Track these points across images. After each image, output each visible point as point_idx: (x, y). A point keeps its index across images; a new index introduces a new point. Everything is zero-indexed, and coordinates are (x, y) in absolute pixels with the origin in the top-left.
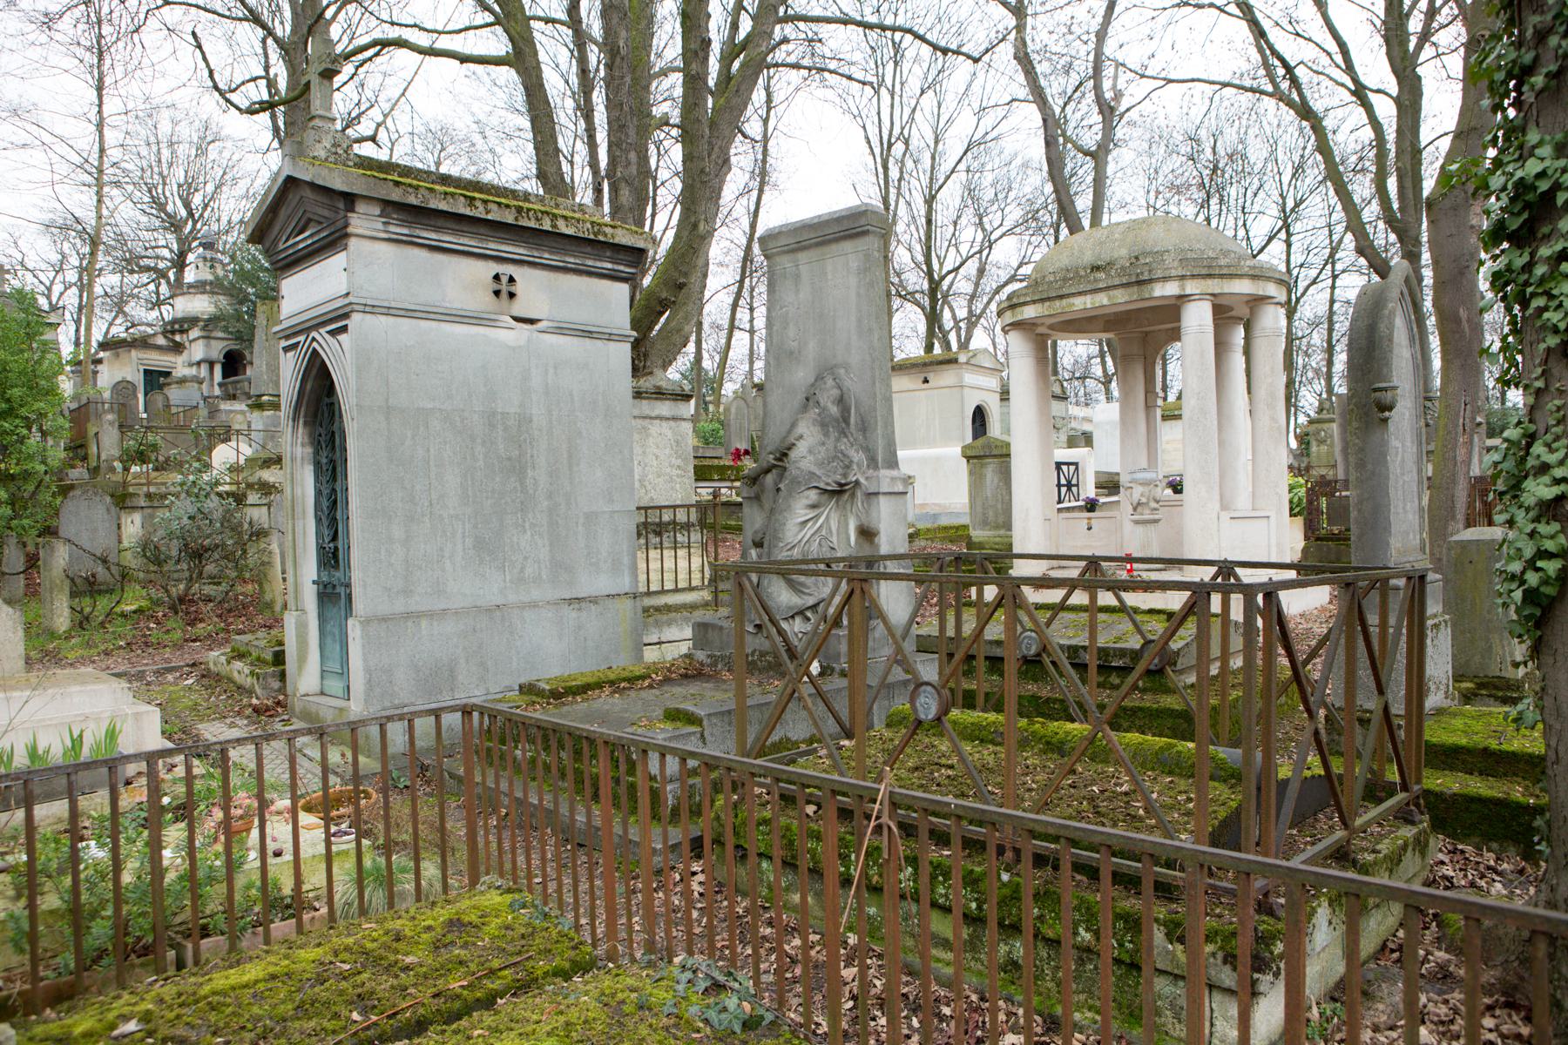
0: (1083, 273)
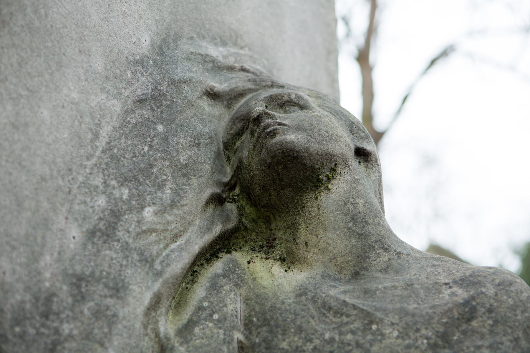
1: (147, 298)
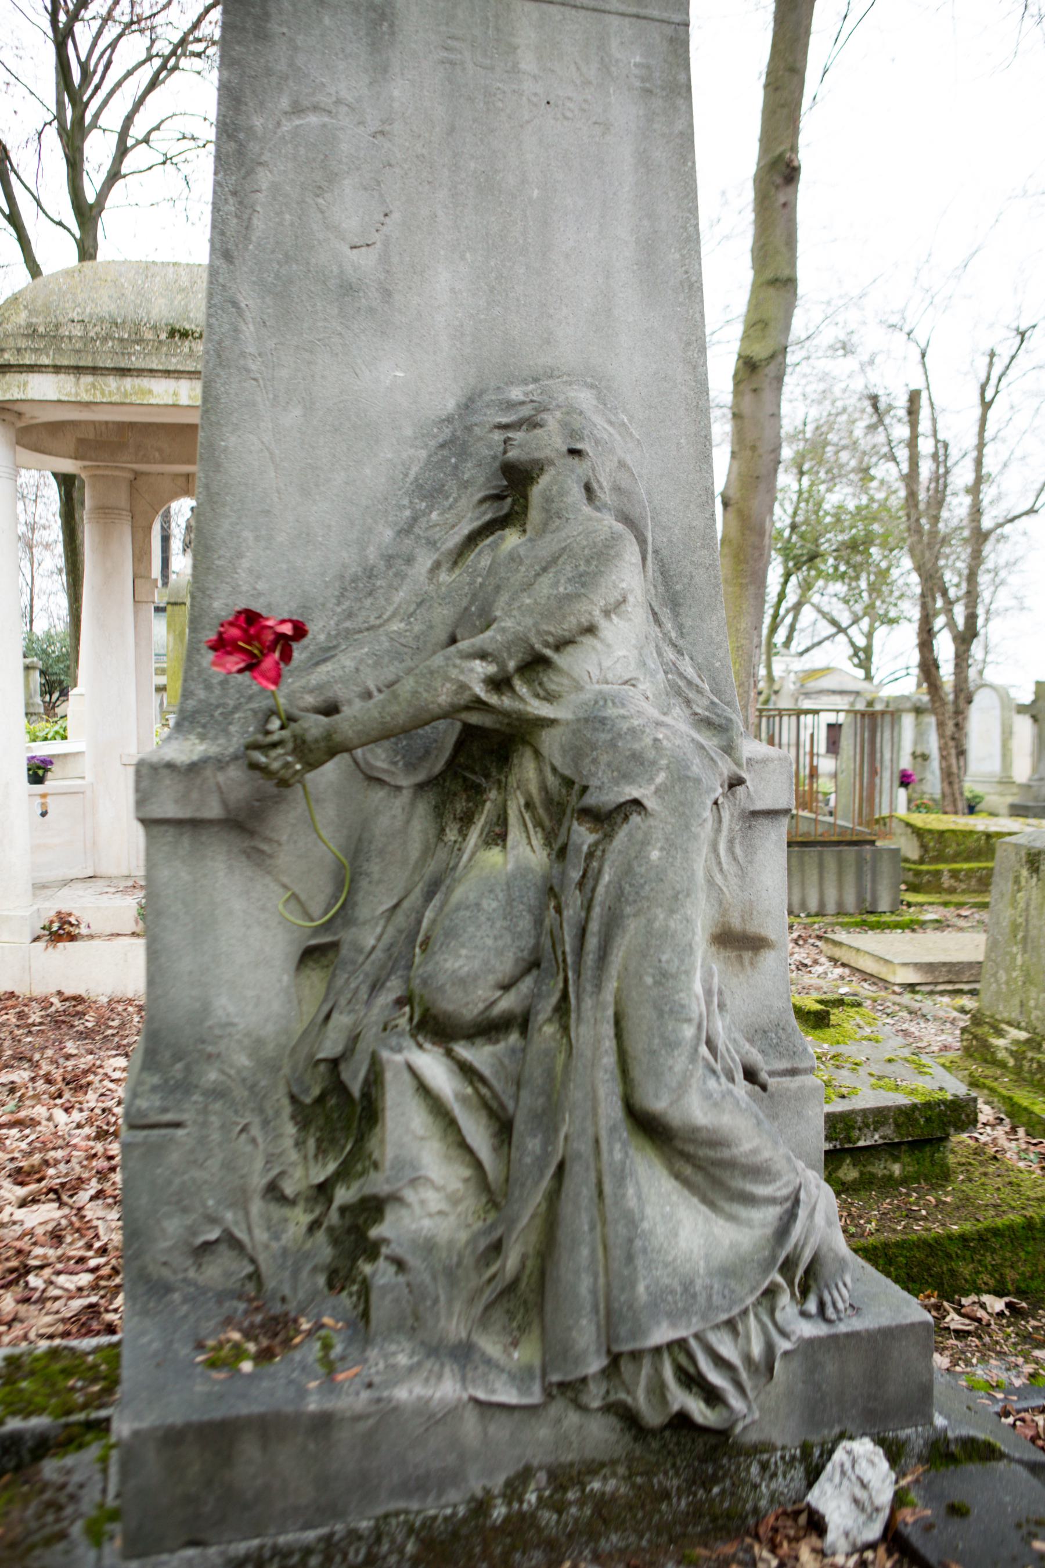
0: (149, 335)
1: (429, 564)
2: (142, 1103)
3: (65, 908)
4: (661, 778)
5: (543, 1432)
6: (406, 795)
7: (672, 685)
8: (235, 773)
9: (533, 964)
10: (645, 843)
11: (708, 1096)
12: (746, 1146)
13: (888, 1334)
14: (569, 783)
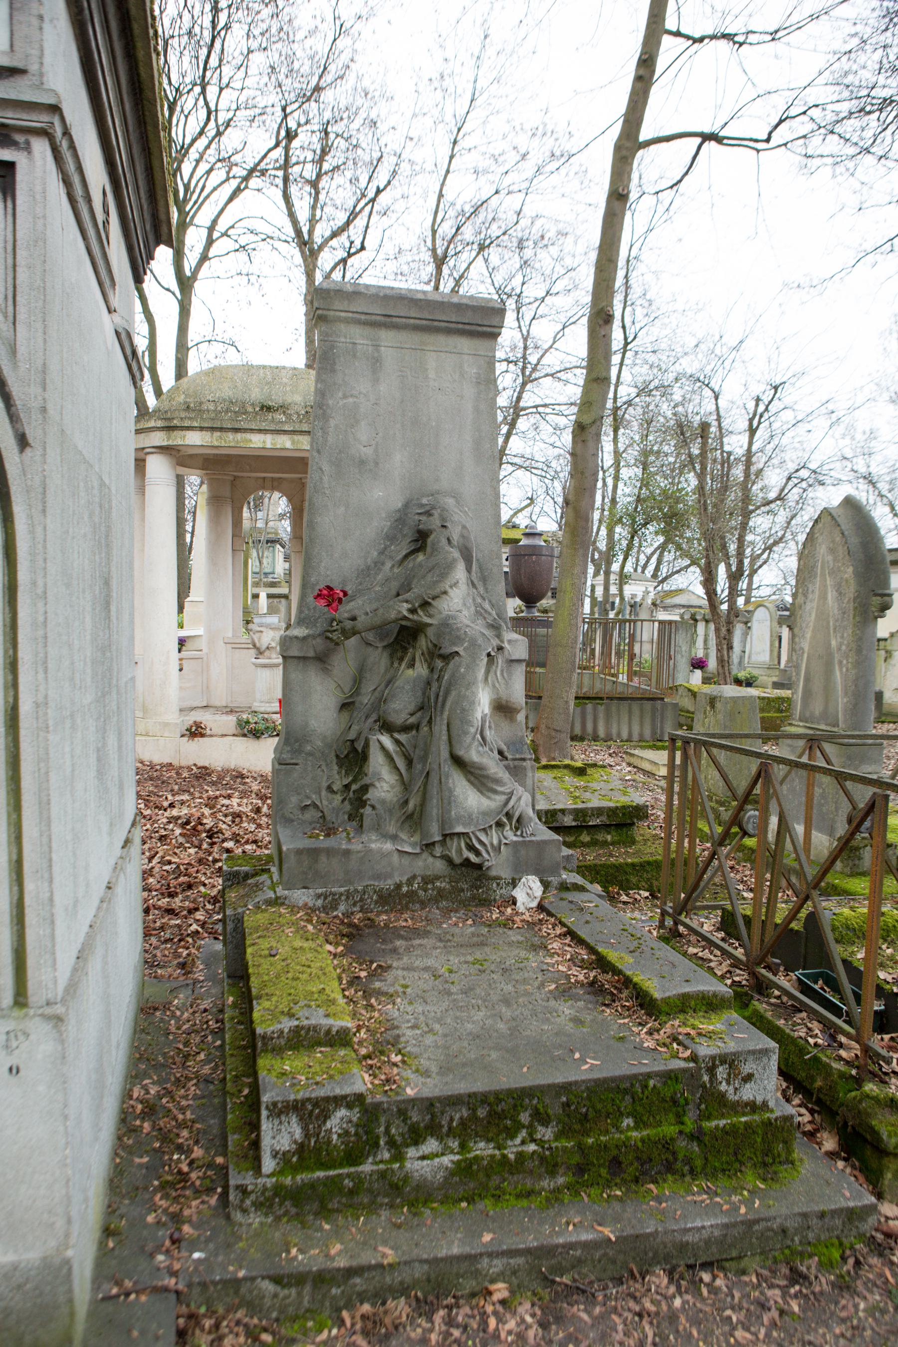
0: (250, 409)
2: (284, 756)
3: (198, 719)
4: (466, 644)
5: (420, 863)
6: (380, 650)
7: (477, 612)
8: (319, 640)
9: (421, 708)
10: (459, 666)
11: (479, 752)
12: (493, 771)
13: (545, 842)
14: (435, 646)
